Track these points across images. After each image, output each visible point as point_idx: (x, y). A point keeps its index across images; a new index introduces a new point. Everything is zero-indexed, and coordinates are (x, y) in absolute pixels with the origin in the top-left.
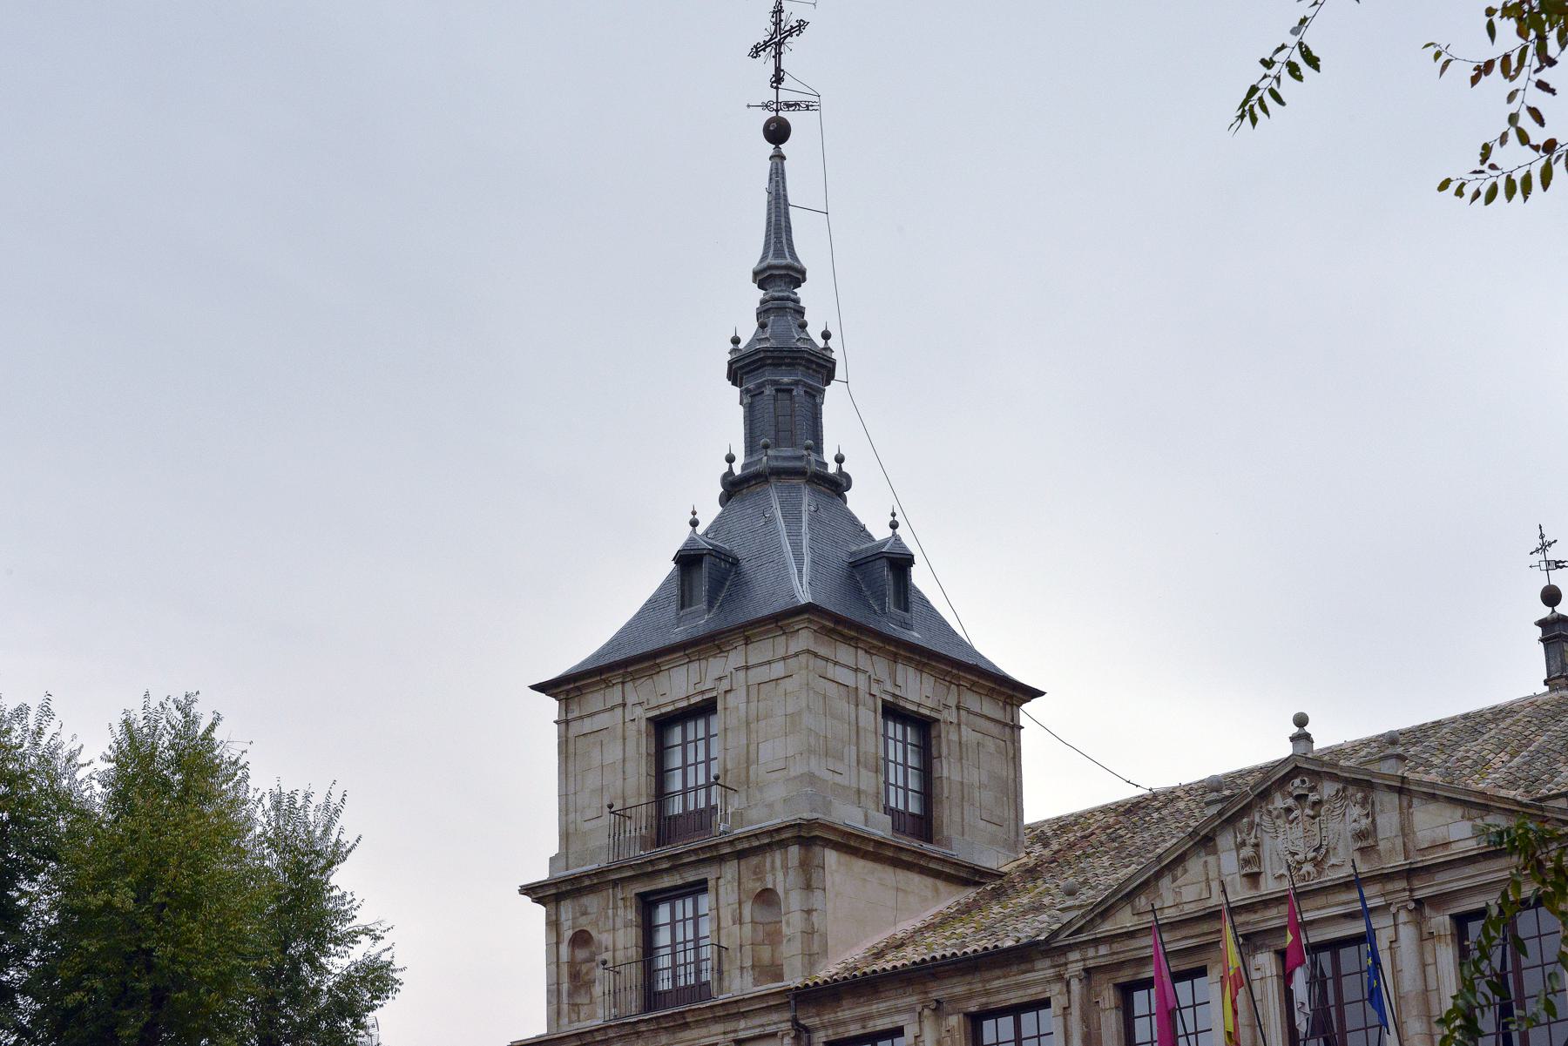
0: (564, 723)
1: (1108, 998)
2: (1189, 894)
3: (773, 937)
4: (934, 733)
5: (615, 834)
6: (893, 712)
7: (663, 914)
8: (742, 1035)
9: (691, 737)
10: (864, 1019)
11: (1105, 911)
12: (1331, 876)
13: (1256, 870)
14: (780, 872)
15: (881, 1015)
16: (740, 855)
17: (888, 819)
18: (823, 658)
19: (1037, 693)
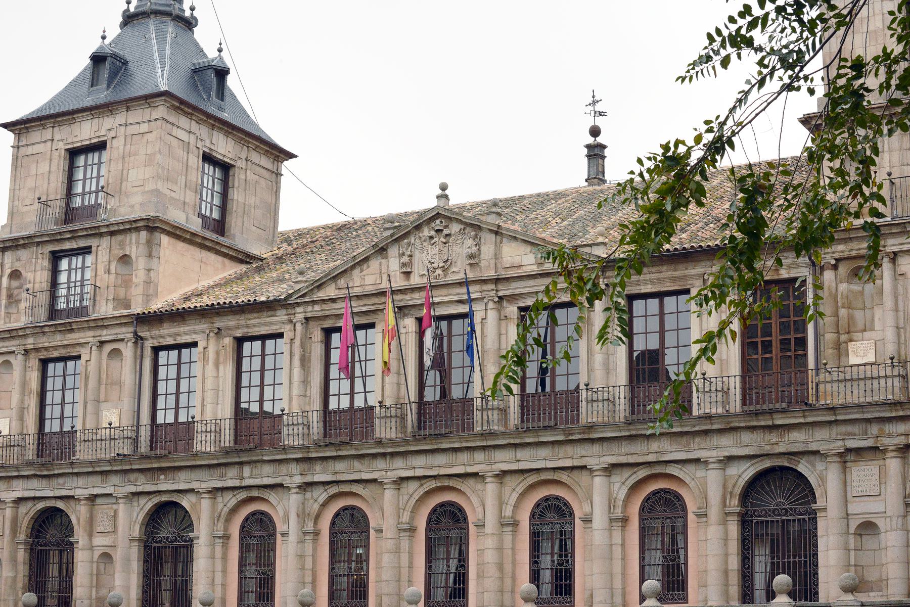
0: (17, 147)
1: (318, 335)
2: (369, 280)
3: (127, 283)
4: (231, 173)
5: (40, 216)
6: (208, 158)
7: (64, 264)
8: (104, 339)
9: (90, 162)
10: (176, 335)
11: (320, 285)
12: (452, 278)
13: (409, 270)
14: (135, 245)
15: (185, 334)
16: (112, 234)
17: (200, 220)
18: (171, 123)
19: (291, 156)
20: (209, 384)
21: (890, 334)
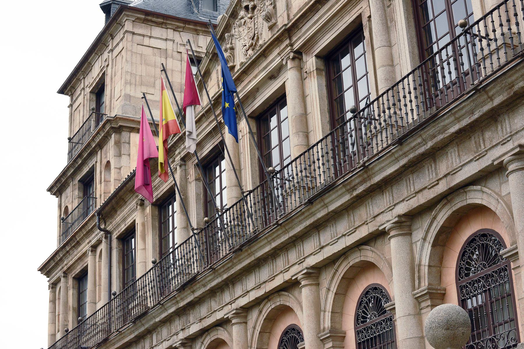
18: (139, 35)
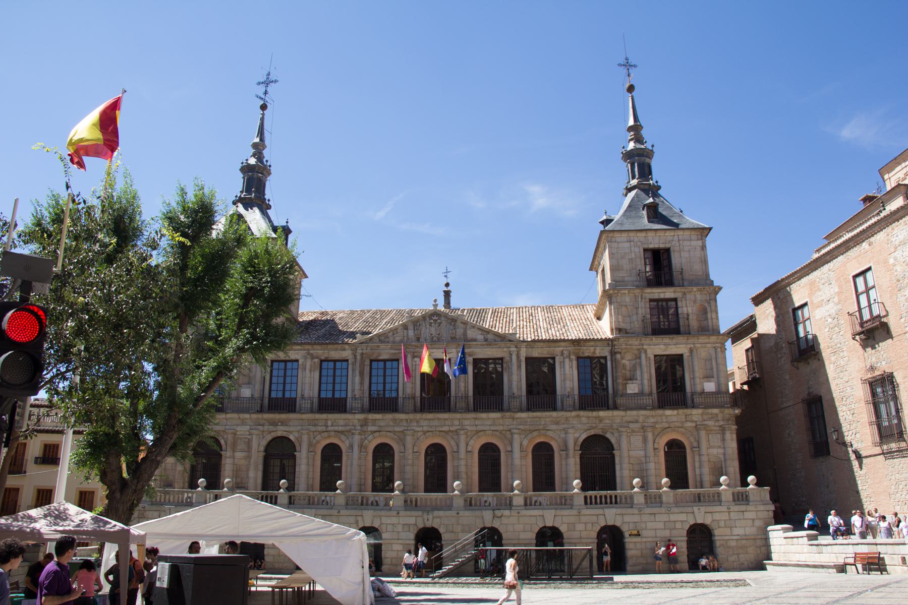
1: (367, 362)
20: (307, 380)
21: (646, 382)
